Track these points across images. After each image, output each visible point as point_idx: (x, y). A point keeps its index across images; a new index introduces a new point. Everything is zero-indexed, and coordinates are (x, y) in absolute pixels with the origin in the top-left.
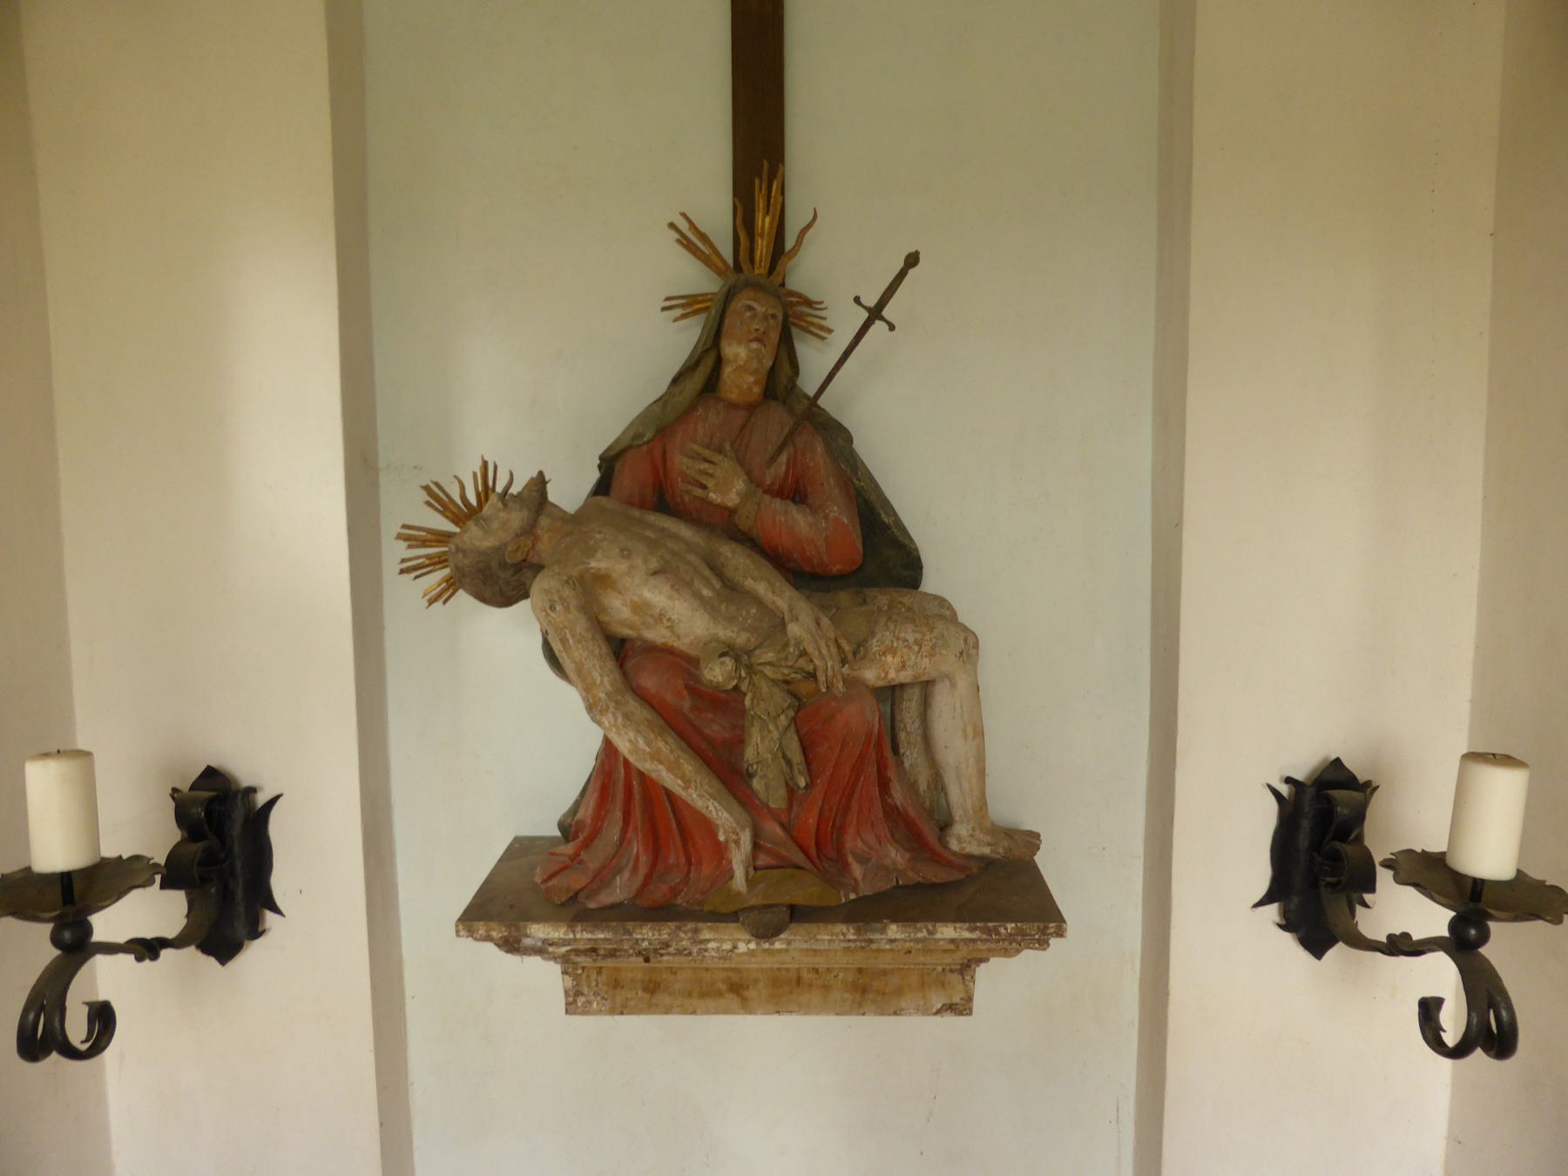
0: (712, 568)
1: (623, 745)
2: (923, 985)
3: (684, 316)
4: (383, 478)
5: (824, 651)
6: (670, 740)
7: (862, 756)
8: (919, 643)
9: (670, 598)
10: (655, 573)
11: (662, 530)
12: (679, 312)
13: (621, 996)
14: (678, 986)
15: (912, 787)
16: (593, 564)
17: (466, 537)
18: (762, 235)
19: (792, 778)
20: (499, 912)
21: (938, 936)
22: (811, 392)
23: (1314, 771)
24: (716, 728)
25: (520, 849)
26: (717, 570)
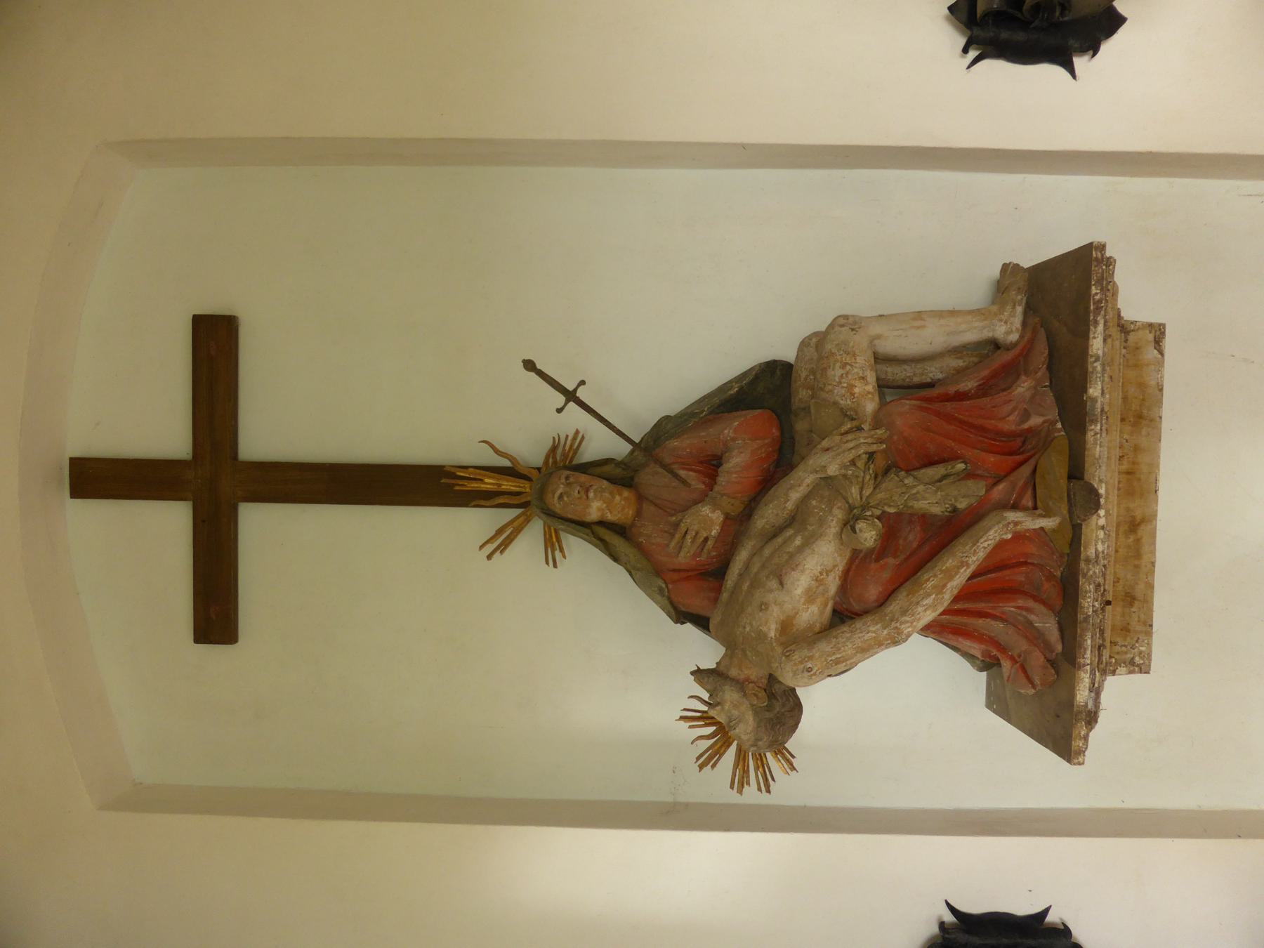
0: (775, 536)
1: (928, 617)
2: (1137, 366)
3: (561, 550)
4: (682, 799)
5: (851, 445)
6: (926, 577)
7: (938, 414)
8: (844, 365)
9: (803, 571)
10: (781, 584)
11: (740, 575)
12: (557, 553)
13: (1135, 626)
14: (1129, 576)
15: (960, 373)
16: (772, 634)
17: (744, 737)
18: (500, 485)
19: (958, 474)
20: (1062, 729)
21: (1100, 353)
22: (629, 447)
23: (956, 27)
24: (911, 537)
25: (998, 703)
26: (777, 531)
